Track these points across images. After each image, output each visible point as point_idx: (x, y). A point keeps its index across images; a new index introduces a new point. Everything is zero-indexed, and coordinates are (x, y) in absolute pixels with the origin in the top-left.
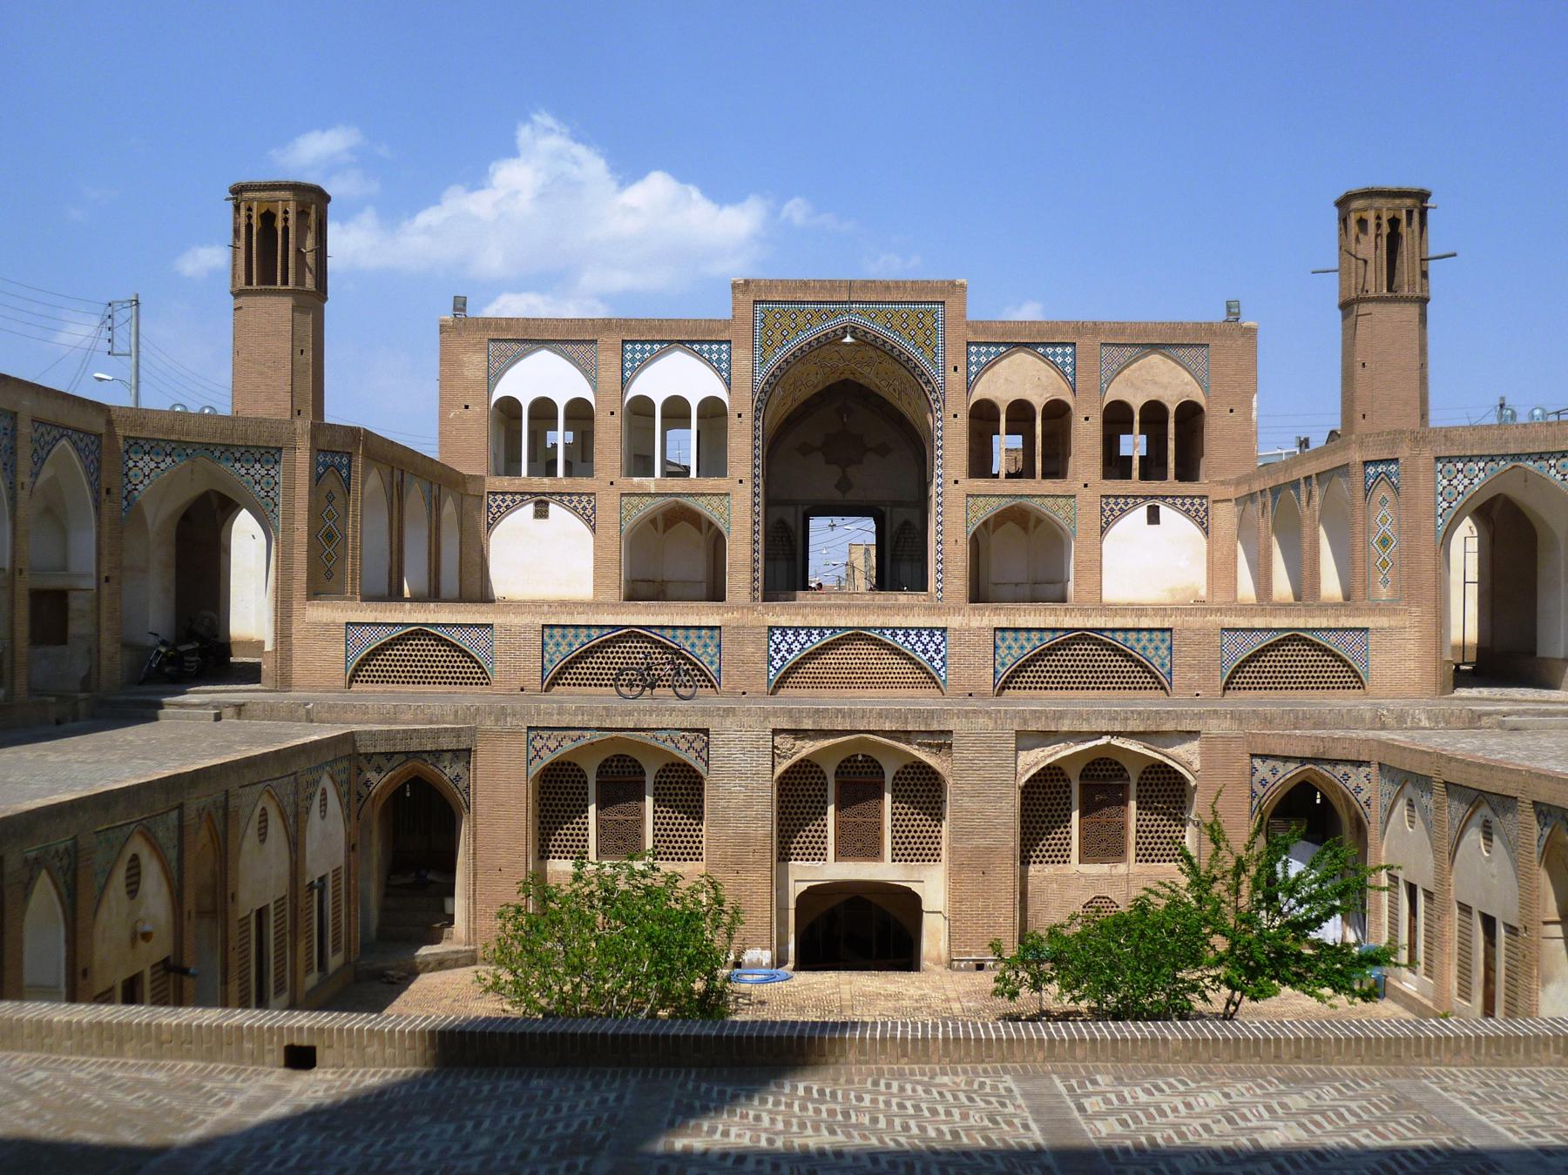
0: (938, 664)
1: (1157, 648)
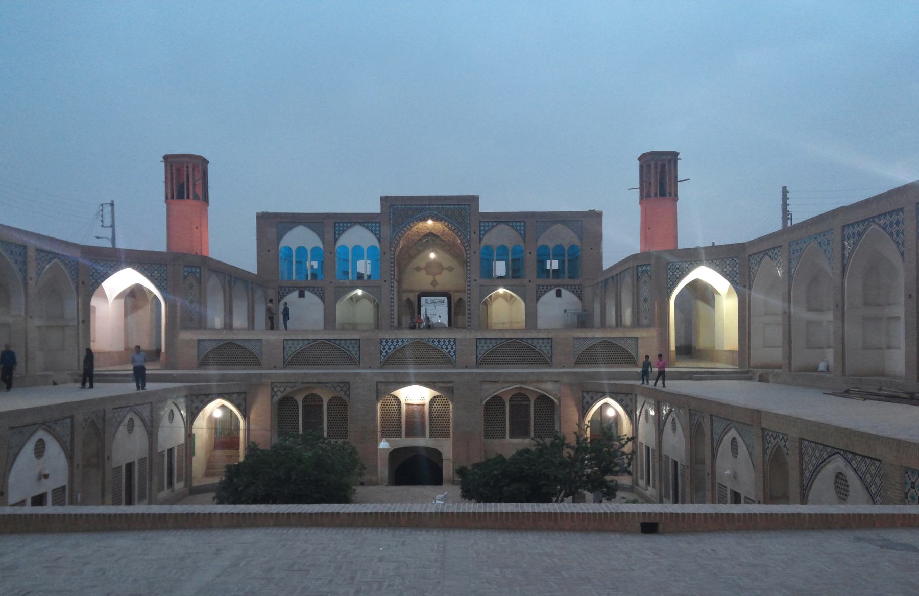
0: (452, 354)
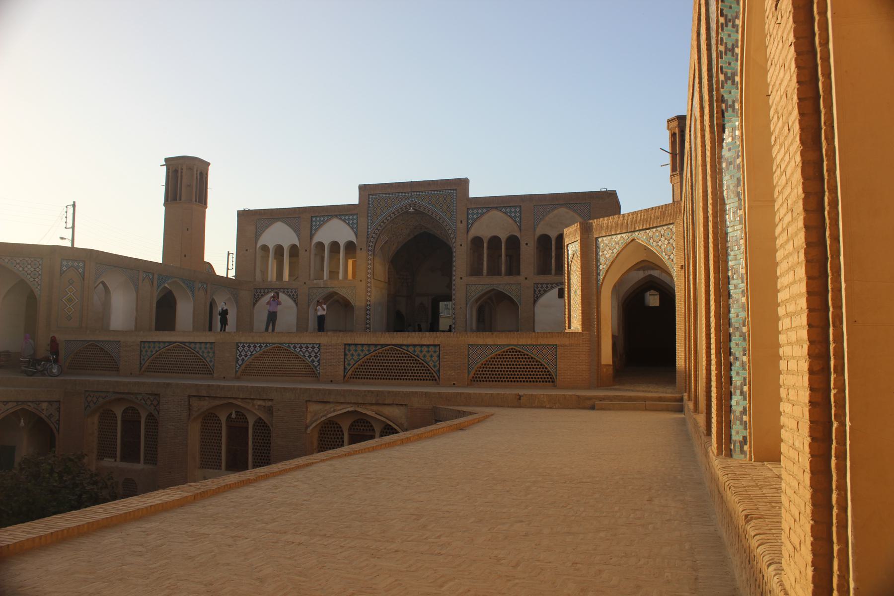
0: (316, 364)
1: (431, 356)
